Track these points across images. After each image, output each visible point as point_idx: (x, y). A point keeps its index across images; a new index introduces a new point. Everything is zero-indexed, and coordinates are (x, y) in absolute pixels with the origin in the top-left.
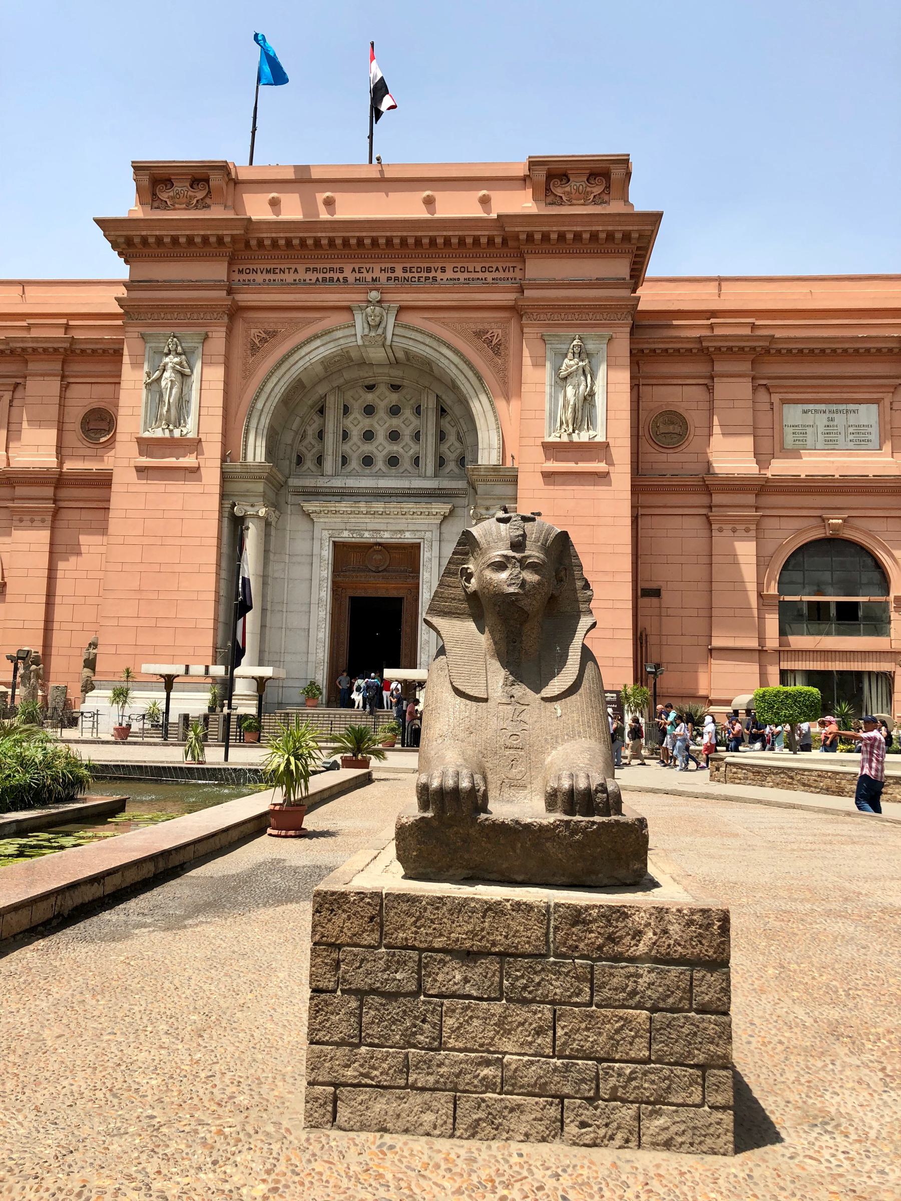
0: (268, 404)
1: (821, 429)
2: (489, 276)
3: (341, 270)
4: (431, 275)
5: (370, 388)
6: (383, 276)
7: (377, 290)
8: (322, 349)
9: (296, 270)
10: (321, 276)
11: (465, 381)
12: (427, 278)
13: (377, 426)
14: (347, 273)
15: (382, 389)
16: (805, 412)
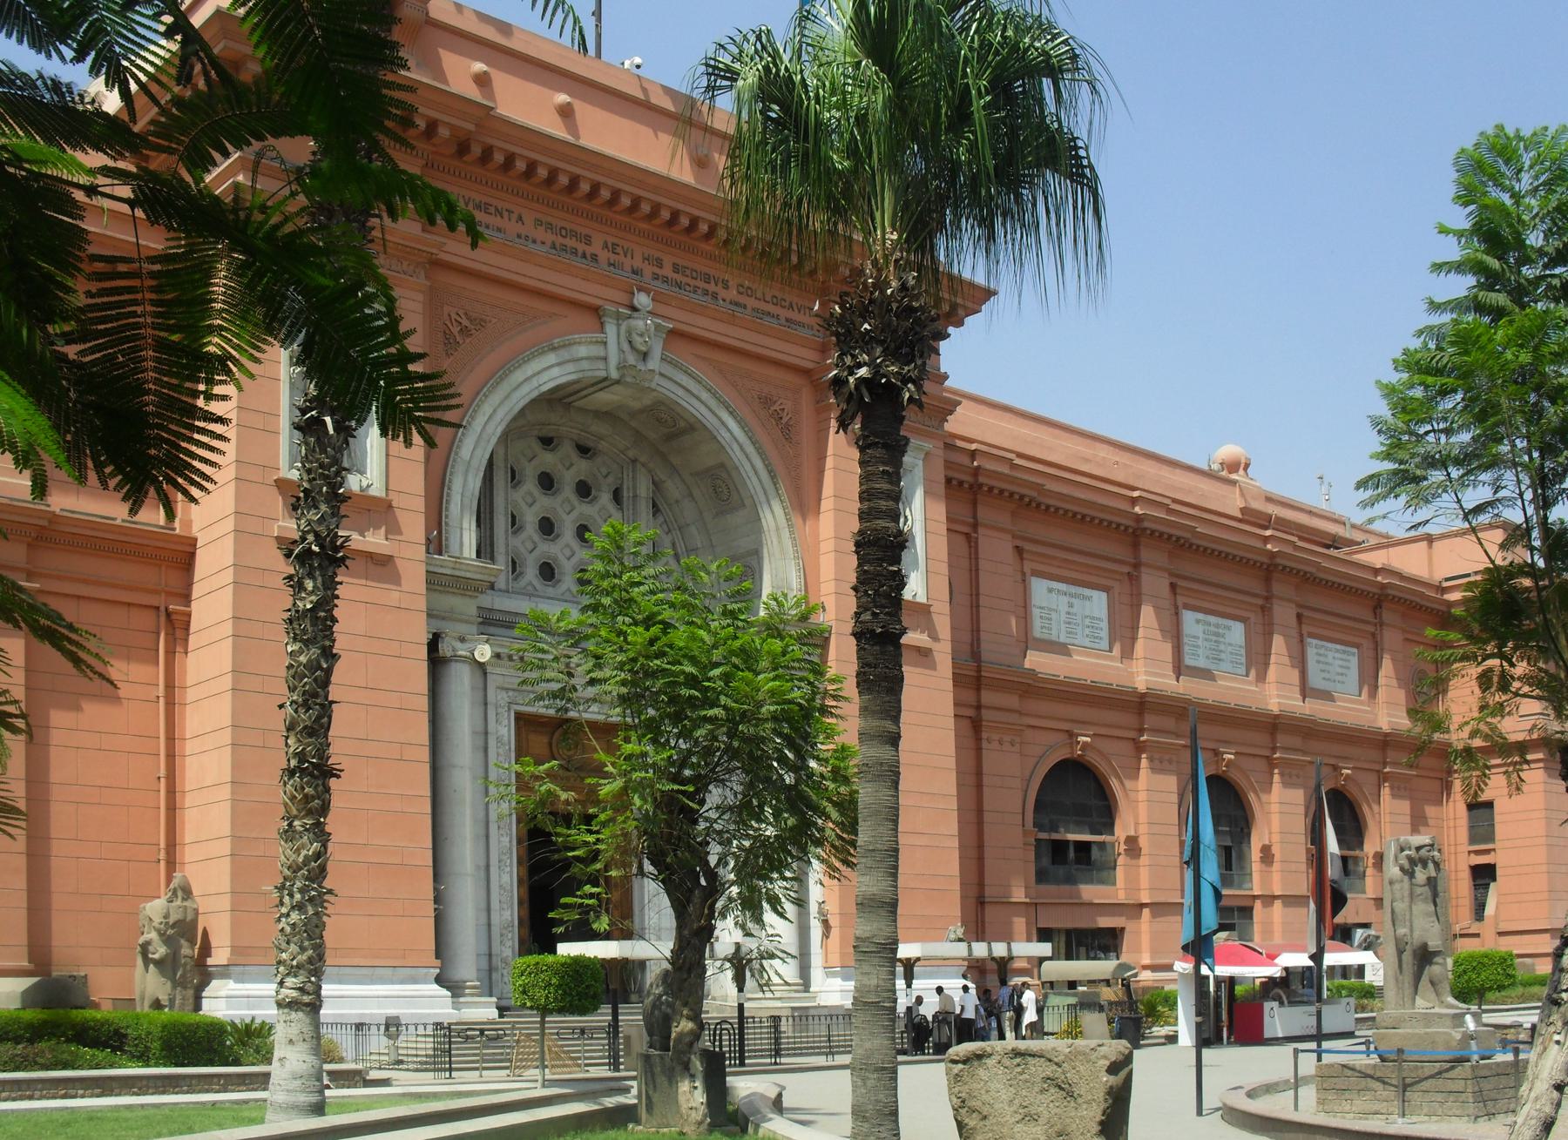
0: (479, 452)
1: (1063, 617)
2: (784, 313)
3: (588, 240)
4: (712, 287)
5: (547, 442)
6: (648, 270)
7: (648, 292)
8: (556, 371)
9: (520, 218)
10: (560, 240)
11: (751, 474)
12: (706, 293)
13: (560, 510)
14: (596, 247)
15: (567, 449)
16: (1050, 590)
